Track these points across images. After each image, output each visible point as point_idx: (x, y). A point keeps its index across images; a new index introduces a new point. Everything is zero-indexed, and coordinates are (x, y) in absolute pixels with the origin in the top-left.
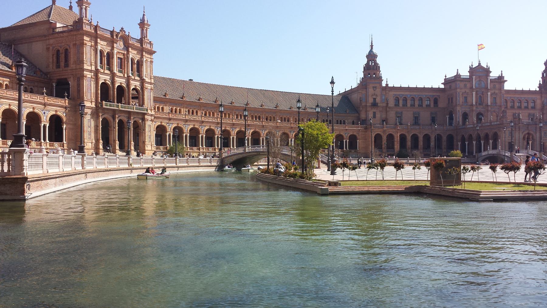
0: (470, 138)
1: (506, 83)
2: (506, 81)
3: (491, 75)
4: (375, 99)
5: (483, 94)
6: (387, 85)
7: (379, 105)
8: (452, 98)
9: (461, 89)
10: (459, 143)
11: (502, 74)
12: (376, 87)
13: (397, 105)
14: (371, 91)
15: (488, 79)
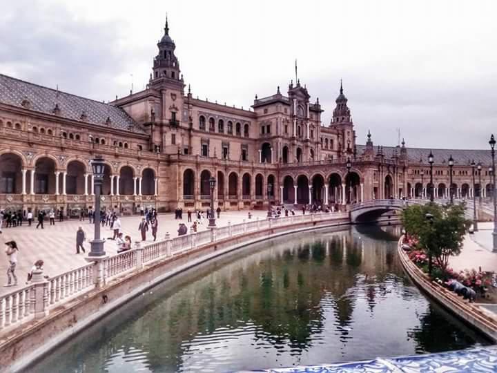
0: (303, 181)
1: (322, 113)
2: (323, 111)
3: (310, 100)
4: (174, 114)
5: (302, 125)
6: (190, 95)
7: (180, 125)
8: (269, 127)
9: (282, 114)
10: (282, 187)
11: (318, 102)
12: (175, 95)
13: (202, 128)
14: (168, 99)
15: (307, 105)
